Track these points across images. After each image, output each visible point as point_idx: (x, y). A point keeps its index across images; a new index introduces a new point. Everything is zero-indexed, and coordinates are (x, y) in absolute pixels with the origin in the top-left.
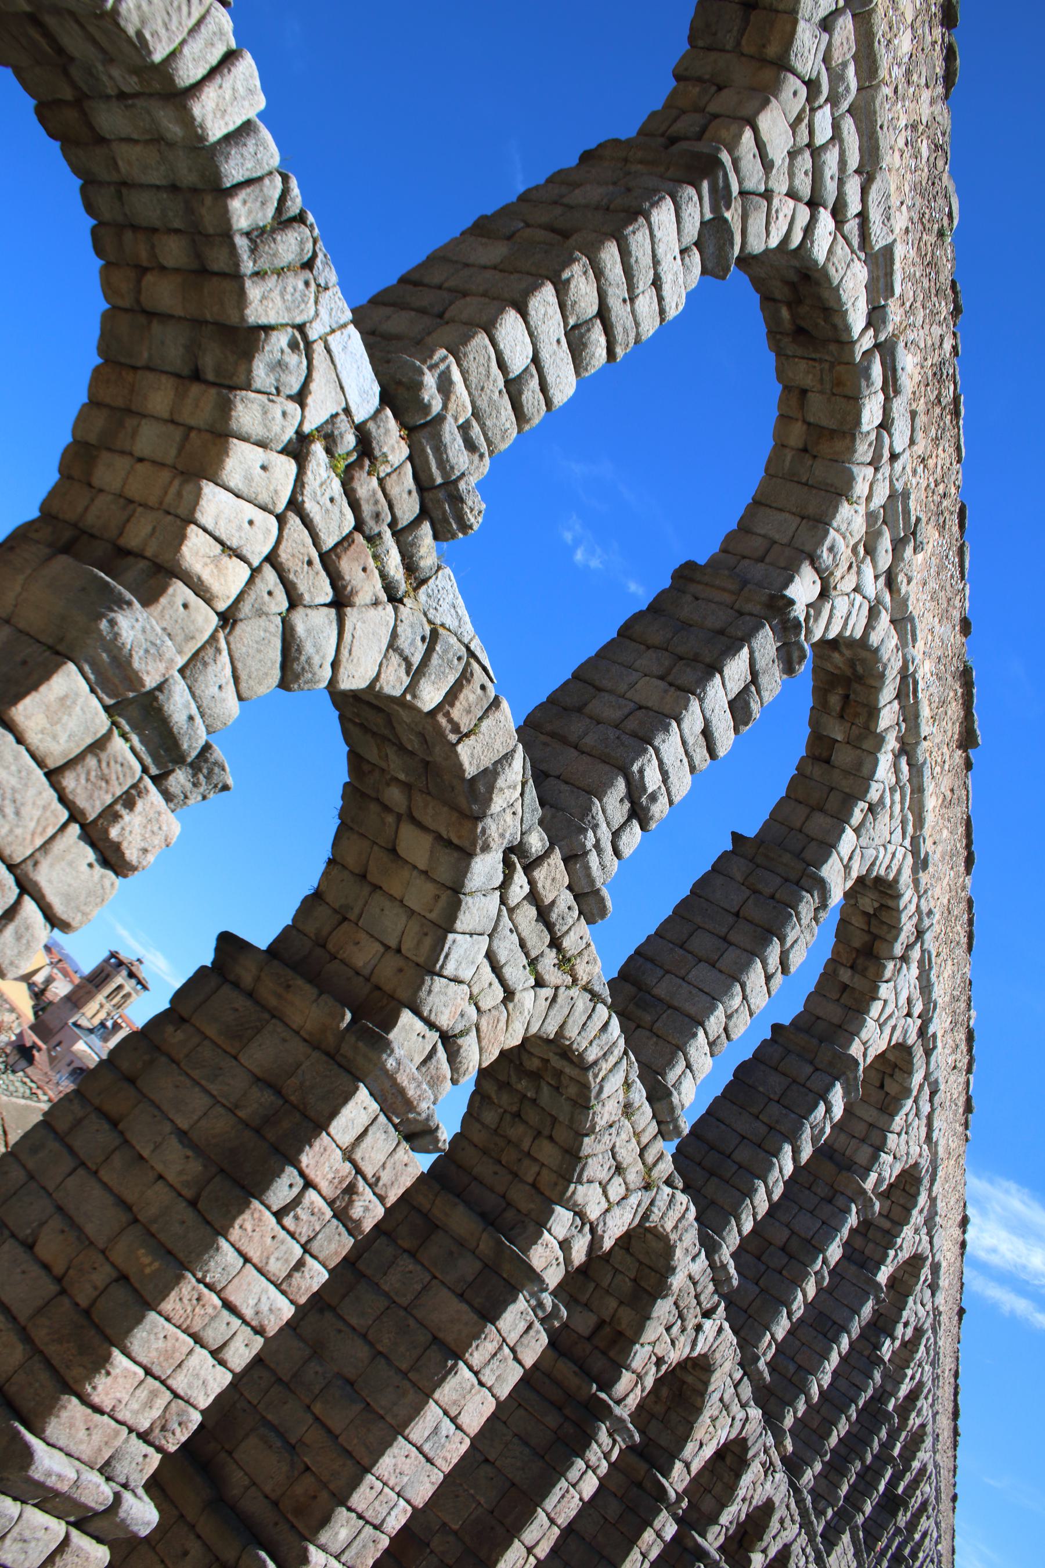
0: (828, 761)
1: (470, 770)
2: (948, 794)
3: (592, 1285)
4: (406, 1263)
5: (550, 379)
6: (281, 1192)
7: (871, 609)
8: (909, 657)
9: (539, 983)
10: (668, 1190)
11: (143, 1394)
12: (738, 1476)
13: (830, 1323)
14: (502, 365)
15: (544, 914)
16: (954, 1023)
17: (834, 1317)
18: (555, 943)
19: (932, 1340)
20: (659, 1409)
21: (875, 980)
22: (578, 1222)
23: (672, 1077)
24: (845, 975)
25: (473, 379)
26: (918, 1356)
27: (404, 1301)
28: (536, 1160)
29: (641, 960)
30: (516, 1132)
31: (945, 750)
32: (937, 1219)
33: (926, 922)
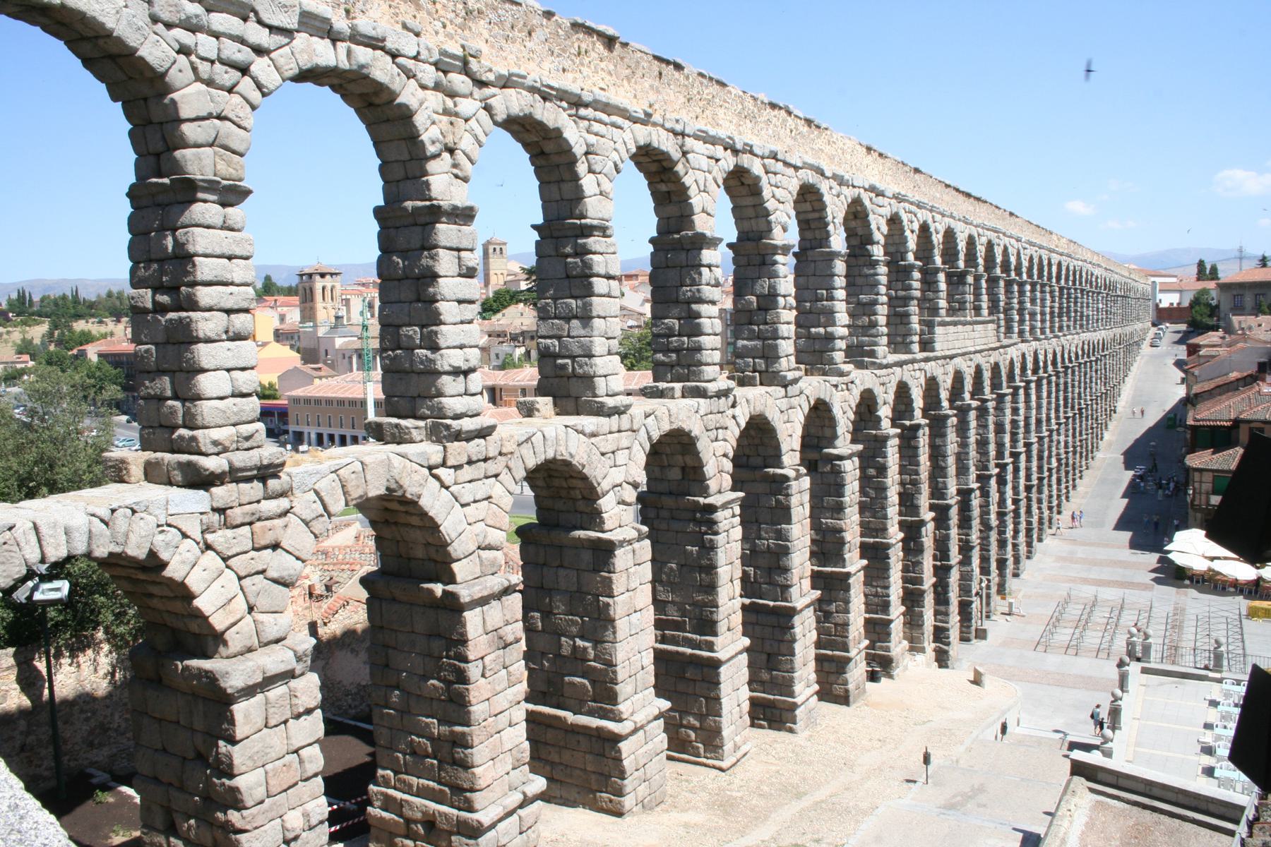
0: (543, 153)
1: (382, 491)
2: (628, 72)
4: (562, 572)
5: (243, 366)
6: (473, 670)
7: (485, 108)
8: (531, 83)
9: (496, 476)
10: (650, 419)
11: (498, 765)
15: (470, 462)
16: (752, 118)
18: (485, 460)
19: (907, 205)
20: (757, 441)
21: (677, 179)
24: (663, 188)
25: (221, 422)
26: (905, 222)
27: (575, 588)
28: (574, 488)
30: (556, 482)
31: (603, 65)
32: (846, 177)
33: (679, 128)
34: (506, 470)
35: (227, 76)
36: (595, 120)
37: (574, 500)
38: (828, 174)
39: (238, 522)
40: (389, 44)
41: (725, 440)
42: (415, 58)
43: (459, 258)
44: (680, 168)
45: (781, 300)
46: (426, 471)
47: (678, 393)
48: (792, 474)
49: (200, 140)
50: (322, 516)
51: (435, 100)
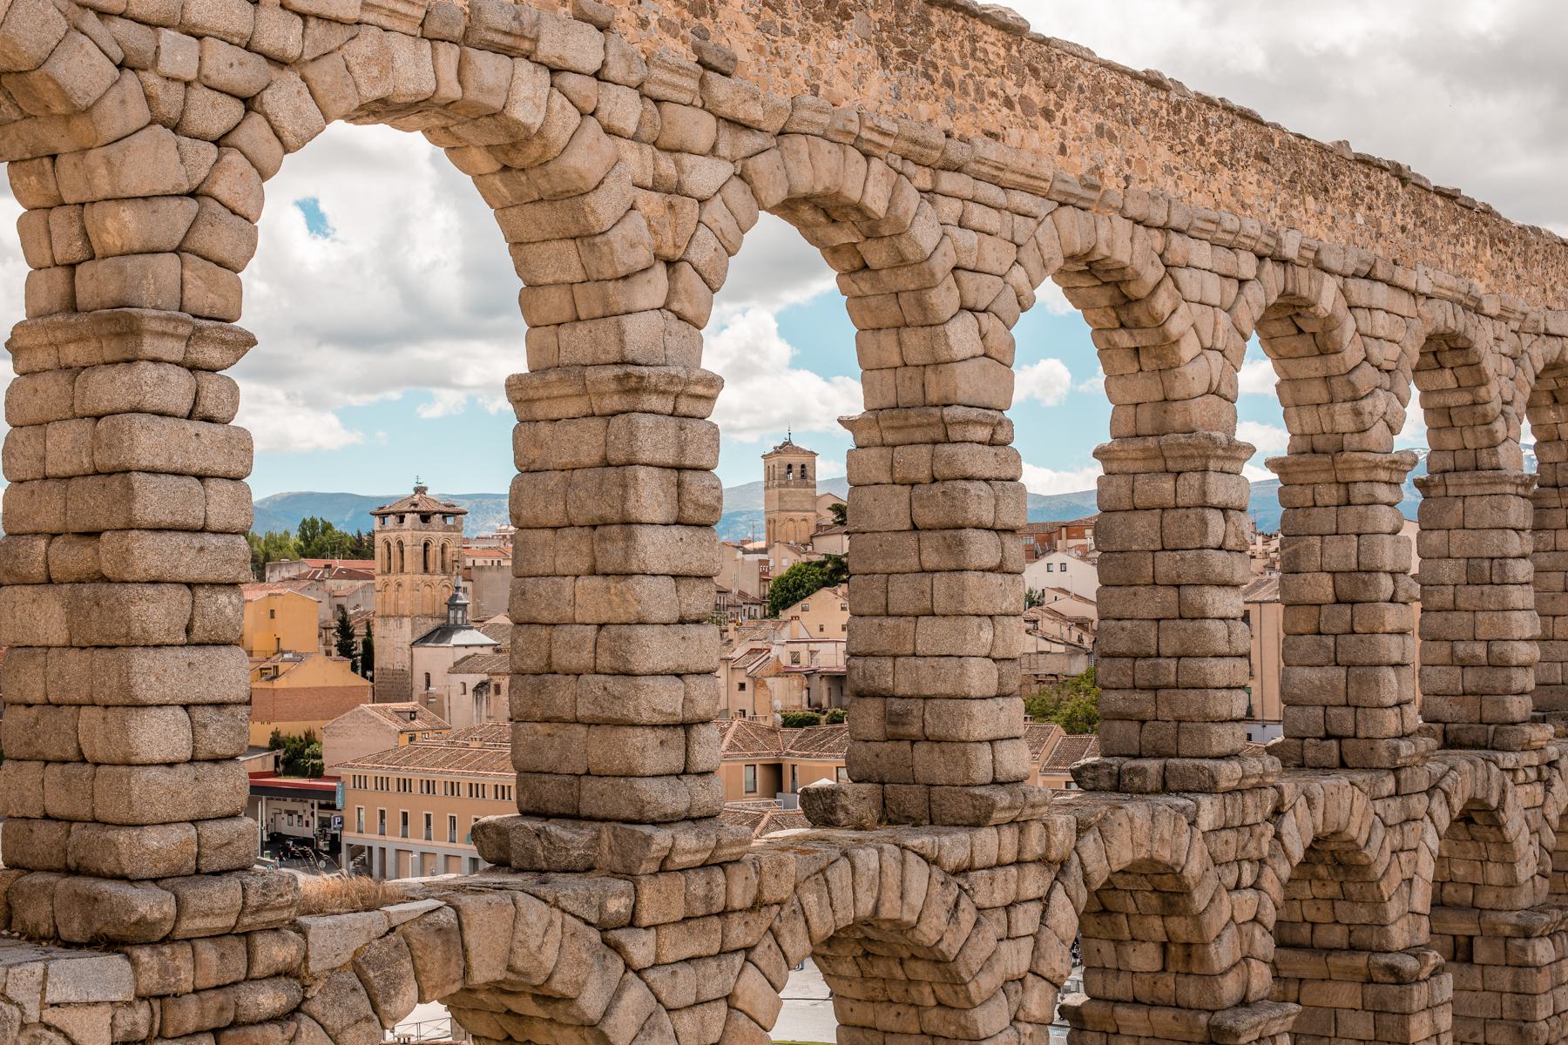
0: (865, 267)
1: (498, 974)
3: (1123, 917)
8: (839, 125)
12: (1500, 827)
13: (1486, 564)
14: (171, 765)
17: (1485, 554)
18: (724, 913)
20: (1332, 889)
21: (1159, 324)
22: (1011, 987)
23: (982, 772)
24: (1124, 339)
29: (859, 662)
30: (879, 969)
31: (992, 84)
33: (1159, 217)
34: (769, 940)
35: (215, 114)
36: (973, 200)
37: (918, 1007)
38: (1491, 307)
39: (190, 1026)
40: (546, 50)
41: (1256, 886)
42: (597, 75)
43: (679, 485)
44: (1163, 303)
45: (1386, 583)
46: (595, 936)
47: (1153, 782)
48: (1410, 964)
49: (156, 242)
50: (368, 1019)
51: (637, 161)
